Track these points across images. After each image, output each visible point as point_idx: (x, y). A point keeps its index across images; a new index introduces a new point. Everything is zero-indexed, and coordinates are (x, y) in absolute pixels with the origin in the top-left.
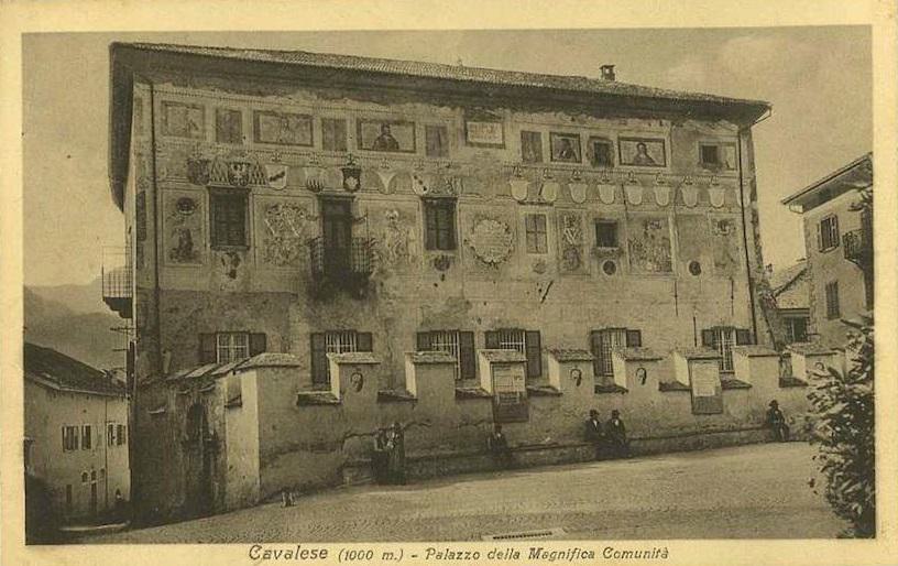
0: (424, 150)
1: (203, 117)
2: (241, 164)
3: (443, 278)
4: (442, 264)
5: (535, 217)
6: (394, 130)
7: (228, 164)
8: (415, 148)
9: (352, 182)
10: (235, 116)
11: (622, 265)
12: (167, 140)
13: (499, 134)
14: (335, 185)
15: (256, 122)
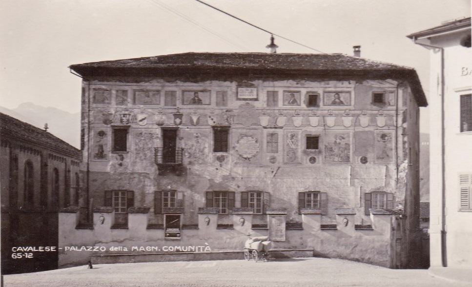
0: (215, 104)
3: (221, 166)
4: (221, 159)
5: (272, 135)
6: (200, 94)
8: (210, 103)
9: (178, 121)
11: (320, 159)
12: (94, 105)
13: (255, 93)
14: (170, 123)
15: (134, 95)
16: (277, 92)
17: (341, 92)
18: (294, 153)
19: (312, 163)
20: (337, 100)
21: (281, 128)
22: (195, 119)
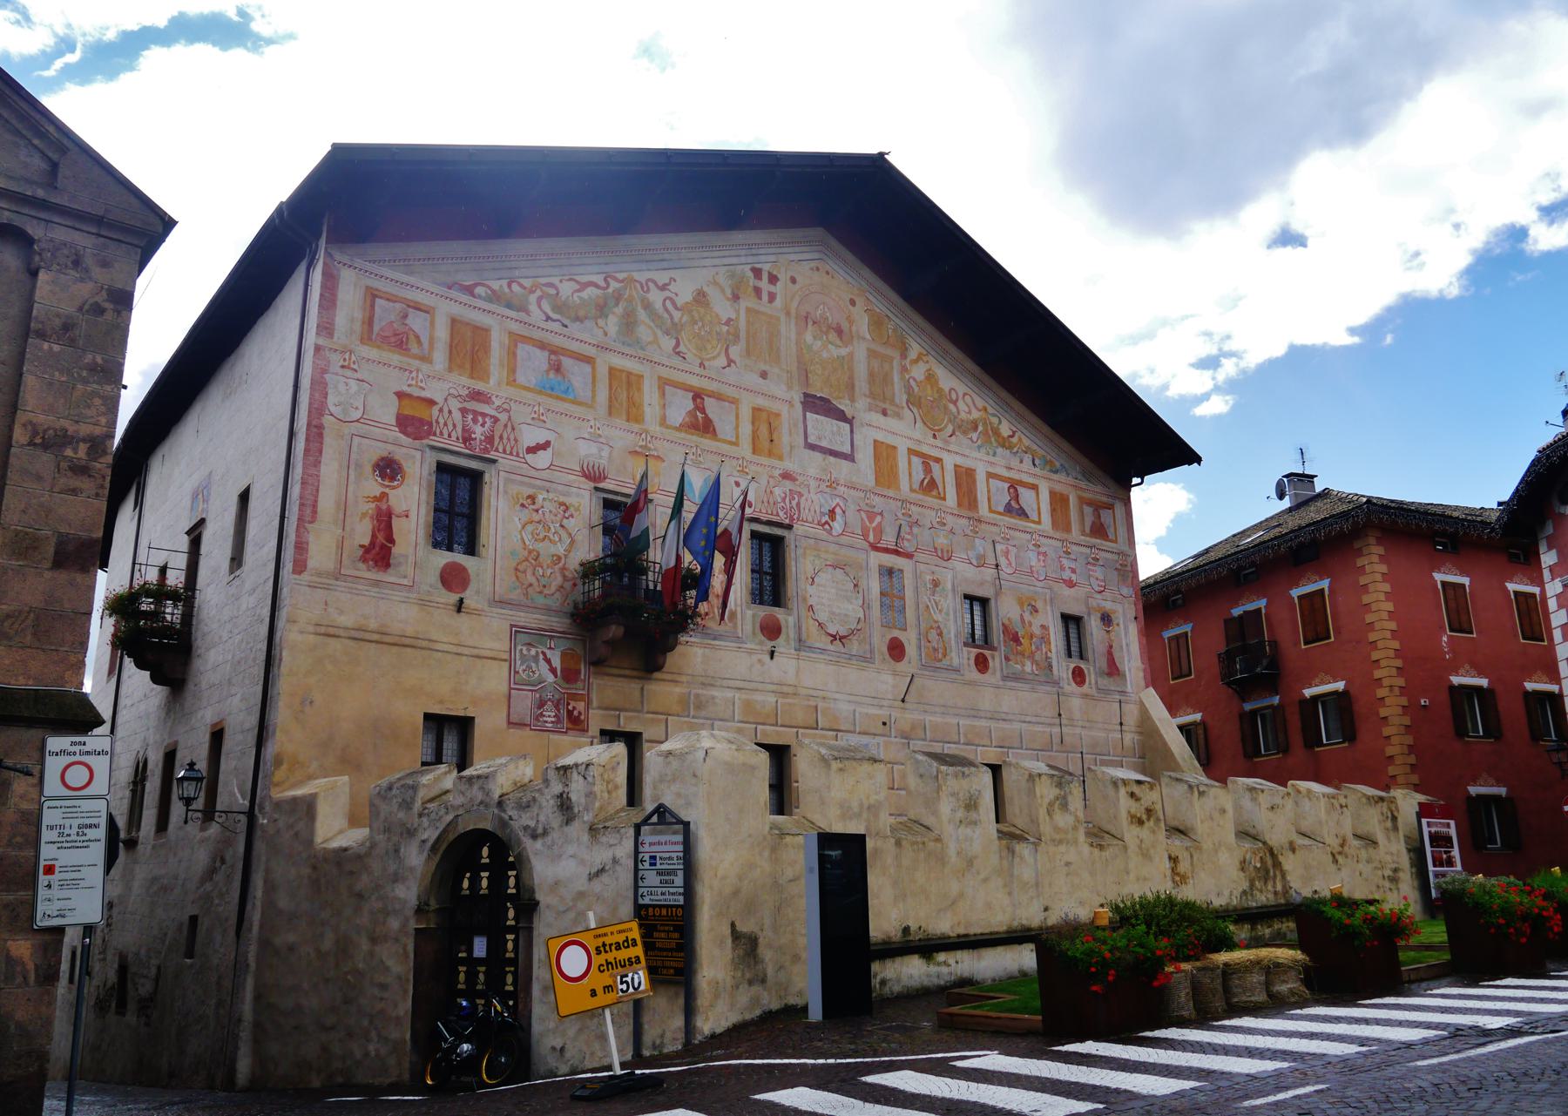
1: (432, 323)
2: (484, 415)
5: (890, 572)
7: (464, 411)
8: (737, 437)
10: (481, 332)
11: (995, 661)
15: (512, 354)
18: (940, 634)
20: (1013, 503)
21: (909, 556)
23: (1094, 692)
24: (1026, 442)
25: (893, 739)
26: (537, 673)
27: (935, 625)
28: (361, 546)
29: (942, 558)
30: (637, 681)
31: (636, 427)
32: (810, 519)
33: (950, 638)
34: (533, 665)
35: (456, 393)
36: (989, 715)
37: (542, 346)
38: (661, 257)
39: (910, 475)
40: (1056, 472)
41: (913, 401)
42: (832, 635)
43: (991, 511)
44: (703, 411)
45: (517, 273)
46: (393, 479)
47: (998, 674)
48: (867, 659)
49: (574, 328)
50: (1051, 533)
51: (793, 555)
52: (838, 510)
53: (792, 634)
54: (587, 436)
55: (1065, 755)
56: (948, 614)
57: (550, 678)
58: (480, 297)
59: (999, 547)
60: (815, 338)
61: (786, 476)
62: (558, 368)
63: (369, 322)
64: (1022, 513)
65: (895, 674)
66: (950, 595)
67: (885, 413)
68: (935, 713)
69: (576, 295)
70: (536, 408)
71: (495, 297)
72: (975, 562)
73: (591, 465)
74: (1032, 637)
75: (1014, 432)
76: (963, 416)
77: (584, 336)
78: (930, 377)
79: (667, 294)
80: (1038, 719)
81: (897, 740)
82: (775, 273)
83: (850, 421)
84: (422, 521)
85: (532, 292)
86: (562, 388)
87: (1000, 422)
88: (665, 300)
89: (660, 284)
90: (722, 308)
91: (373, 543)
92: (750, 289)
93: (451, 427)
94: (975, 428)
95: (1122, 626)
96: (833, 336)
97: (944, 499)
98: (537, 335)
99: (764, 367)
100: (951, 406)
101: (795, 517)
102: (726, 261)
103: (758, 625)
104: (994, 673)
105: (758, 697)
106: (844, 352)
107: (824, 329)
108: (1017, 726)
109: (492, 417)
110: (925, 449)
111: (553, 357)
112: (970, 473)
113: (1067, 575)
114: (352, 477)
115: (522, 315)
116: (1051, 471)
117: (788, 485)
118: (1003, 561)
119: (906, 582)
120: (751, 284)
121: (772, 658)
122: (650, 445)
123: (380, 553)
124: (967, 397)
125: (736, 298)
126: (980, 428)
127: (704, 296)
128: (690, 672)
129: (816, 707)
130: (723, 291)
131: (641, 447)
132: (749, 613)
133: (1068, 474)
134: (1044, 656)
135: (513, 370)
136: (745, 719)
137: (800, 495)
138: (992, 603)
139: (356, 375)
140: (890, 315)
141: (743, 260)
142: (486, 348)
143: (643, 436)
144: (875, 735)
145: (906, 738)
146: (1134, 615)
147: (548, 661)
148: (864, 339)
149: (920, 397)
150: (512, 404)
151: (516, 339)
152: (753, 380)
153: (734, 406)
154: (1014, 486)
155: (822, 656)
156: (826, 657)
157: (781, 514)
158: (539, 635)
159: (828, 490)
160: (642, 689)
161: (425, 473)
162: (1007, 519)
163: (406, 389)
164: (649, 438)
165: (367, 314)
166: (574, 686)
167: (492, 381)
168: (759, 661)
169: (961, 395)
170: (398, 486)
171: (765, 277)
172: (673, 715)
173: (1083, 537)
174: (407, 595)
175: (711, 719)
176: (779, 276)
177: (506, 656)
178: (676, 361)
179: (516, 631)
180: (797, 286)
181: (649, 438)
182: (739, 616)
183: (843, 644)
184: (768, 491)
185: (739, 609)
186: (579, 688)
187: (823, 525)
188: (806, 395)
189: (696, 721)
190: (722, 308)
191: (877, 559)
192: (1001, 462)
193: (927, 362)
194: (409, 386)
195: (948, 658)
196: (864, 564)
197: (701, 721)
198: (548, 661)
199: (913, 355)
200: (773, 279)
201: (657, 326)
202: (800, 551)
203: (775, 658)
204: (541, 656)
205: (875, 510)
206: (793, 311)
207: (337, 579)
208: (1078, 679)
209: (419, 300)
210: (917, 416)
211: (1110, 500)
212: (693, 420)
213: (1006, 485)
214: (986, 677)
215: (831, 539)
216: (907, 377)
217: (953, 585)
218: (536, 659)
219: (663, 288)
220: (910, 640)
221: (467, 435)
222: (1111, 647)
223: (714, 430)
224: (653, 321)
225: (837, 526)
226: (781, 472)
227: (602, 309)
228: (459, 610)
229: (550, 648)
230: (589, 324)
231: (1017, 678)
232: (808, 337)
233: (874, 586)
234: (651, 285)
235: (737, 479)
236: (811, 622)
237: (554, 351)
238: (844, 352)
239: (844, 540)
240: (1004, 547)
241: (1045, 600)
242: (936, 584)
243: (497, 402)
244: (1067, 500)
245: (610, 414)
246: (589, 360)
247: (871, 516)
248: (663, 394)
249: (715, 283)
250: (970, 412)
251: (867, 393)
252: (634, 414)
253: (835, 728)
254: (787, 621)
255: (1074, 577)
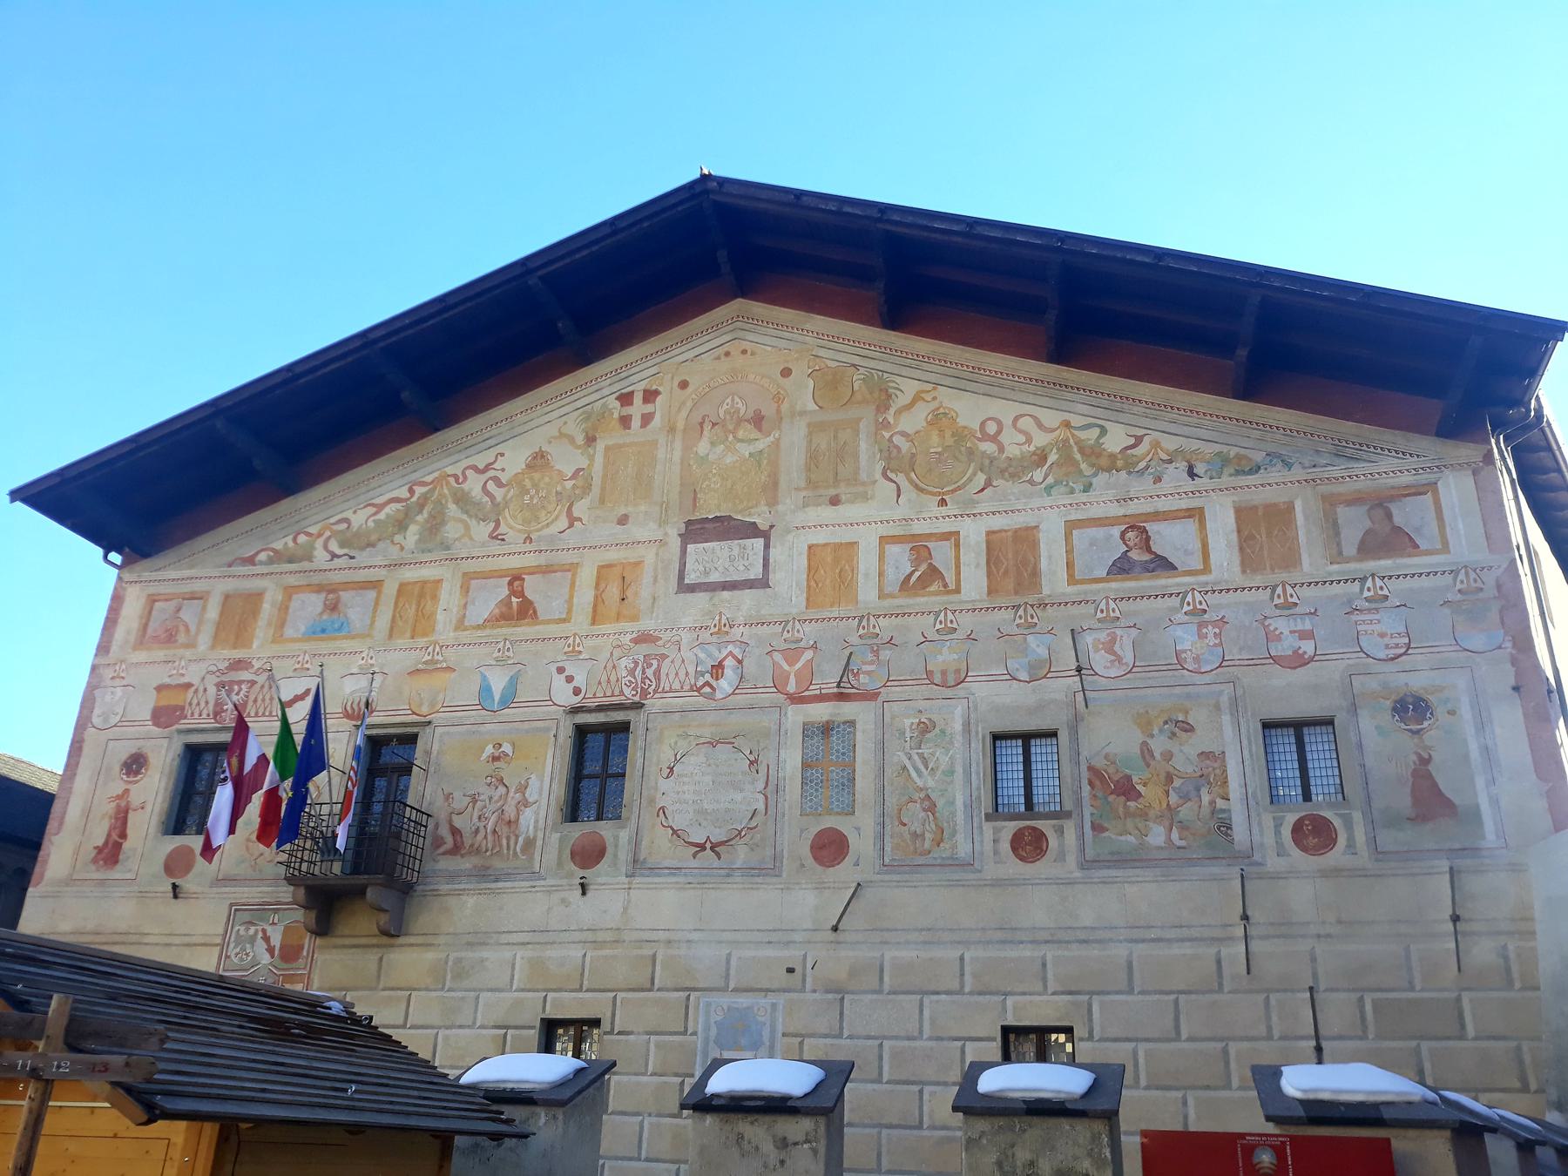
1: (204, 608)
2: (240, 683)
5: (827, 729)
8: (570, 611)
11: (1064, 840)
15: (284, 608)
16: (853, 544)
17: (1157, 516)
18: (931, 808)
19: (1022, 859)
20: (1136, 555)
21: (871, 696)
22: (498, 683)
23: (1364, 858)
24: (1171, 444)
25: (810, 996)
26: (252, 954)
27: (916, 796)
28: (95, 848)
29: (944, 685)
30: (375, 950)
31: (421, 642)
32: (676, 686)
33: (953, 814)
34: (248, 946)
35: (215, 669)
36: (1045, 935)
37: (319, 588)
38: (487, 436)
39: (881, 574)
40: (1256, 469)
41: (895, 463)
42: (697, 845)
43: (1072, 580)
44: (521, 594)
45: (304, 523)
46: (137, 773)
47: (1072, 859)
48: (767, 870)
49: (363, 557)
50: (1238, 579)
51: (640, 743)
52: (729, 662)
53: (624, 855)
54: (355, 670)
55: (1261, 998)
56: (951, 772)
57: (266, 959)
58: (261, 563)
59: (1088, 639)
60: (713, 444)
61: (643, 638)
62: (333, 607)
63: (145, 627)
64: (1163, 564)
65: (820, 887)
66: (959, 740)
67: (835, 501)
68: (908, 942)
69: (372, 518)
70: (300, 659)
71: (278, 557)
72: (1024, 676)
73: (356, 703)
74: (1169, 779)
75: (1139, 440)
76: (1013, 451)
77: (379, 560)
78: (938, 419)
79: (491, 473)
80: (1185, 933)
81: (817, 996)
82: (654, 387)
83: (766, 535)
84: (157, 809)
85: (320, 535)
86: (336, 626)
87: (1104, 431)
88: (486, 482)
89: (481, 466)
90: (567, 460)
91: (106, 843)
92: (615, 424)
93: (203, 705)
94: (1043, 459)
95: (1466, 712)
96: (746, 431)
97: (958, 591)
98: (316, 579)
99: (623, 511)
100: (989, 447)
101: (650, 690)
102: (579, 404)
103: (567, 852)
104: (1061, 857)
105: (552, 953)
106: (762, 444)
107: (731, 427)
108: (1120, 951)
109: (248, 682)
110: (918, 528)
111: (331, 596)
112: (1026, 538)
113: (1283, 648)
114: (100, 782)
115: (306, 565)
116: (1238, 473)
117: (644, 649)
118: (1100, 661)
119: (859, 736)
120: (616, 415)
121: (584, 893)
122: (440, 658)
123: (110, 853)
124: (1025, 423)
125: (591, 440)
126: (1053, 457)
127: (543, 456)
128: (451, 930)
129: (654, 958)
130: (572, 440)
131: (426, 663)
132: (556, 836)
133: (1288, 465)
134: (1206, 810)
135: (282, 624)
136: (528, 986)
137: (664, 657)
138: (1063, 736)
139: (124, 683)
140: (857, 360)
141: (606, 392)
142: (255, 613)
143: (430, 649)
144: (768, 990)
145: (836, 992)
146: (1512, 682)
147: (266, 939)
148: (803, 413)
149: (913, 455)
150: (275, 663)
151: (290, 591)
152: (610, 531)
153: (569, 575)
154: (1137, 528)
155: (674, 879)
156: (681, 879)
157: (627, 691)
158: (262, 910)
159: (714, 639)
160: (381, 959)
161: (168, 760)
162: (1114, 585)
163: (167, 681)
164: (438, 649)
165: (144, 621)
166: (294, 965)
167: (254, 646)
168: (563, 901)
169: (1008, 422)
170: (142, 779)
171: (638, 399)
172: (419, 990)
173: (1335, 567)
174: (128, 889)
175: (475, 990)
176: (660, 389)
177: (218, 940)
178: (496, 547)
179: (236, 910)
180: (690, 389)
181: (438, 649)
182: (539, 843)
183: (718, 855)
184: (610, 665)
185: (540, 835)
186: (300, 967)
187: (698, 690)
188: (689, 523)
189: (453, 994)
190: (567, 460)
191: (796, 716)
192: (1104, 498)
193: (934, 398)
194: (170, 676)
195: (945, 845)
196: (774, 727)
197: (460, 994)
198: (266, 939)
199: (902, 400)
200: (650, 396)
201: (470, 516)
202: (652, 736)
203: (589, 894)
204: (260, 935)
205: (802, 644)
206: (680, 425)
207: (67, 885)
208: (1312, 841)
209: (196, 589)
210: (904, 484)
211: (1425, 478)
212: (504, 609)
213: (1116, 531)
214: (1042, 868)
215: (714, 704)
216: (887, 435)
217: (967, 725)
218: (252, 940)
219: (487, 468)
220: (861, 833)
221: (218, 709)
222: (1425, 761)
223: (535, 612)
224: (467, 512)
225: (725, 685)
226: (635, 635)
227: (401, 525)
228: (176, 897)
229: (273, 924)
230: (381, 545)
231: (1122, 860)
232: (703, 447)
233: (792, 759)
234: (469, 473)
235: (560, 664)
236: (660, 830)
237: (331, 589)
238: (762, 444)
239: (739, 699)
240: (1103, 636)
241: (1217, 707)
242: (925, 729)
243: (257, 665)
244: (1290, 508)
245: (390, 636)
246: (376, 585)
247: (792, 655)
248: (465, 589)
249: (562, 435)
250: (1029, 441)
251: (803, 484)
252: (422, 624)
253: (688, 984)
254: (616, 838)
255: (1308, 647)
